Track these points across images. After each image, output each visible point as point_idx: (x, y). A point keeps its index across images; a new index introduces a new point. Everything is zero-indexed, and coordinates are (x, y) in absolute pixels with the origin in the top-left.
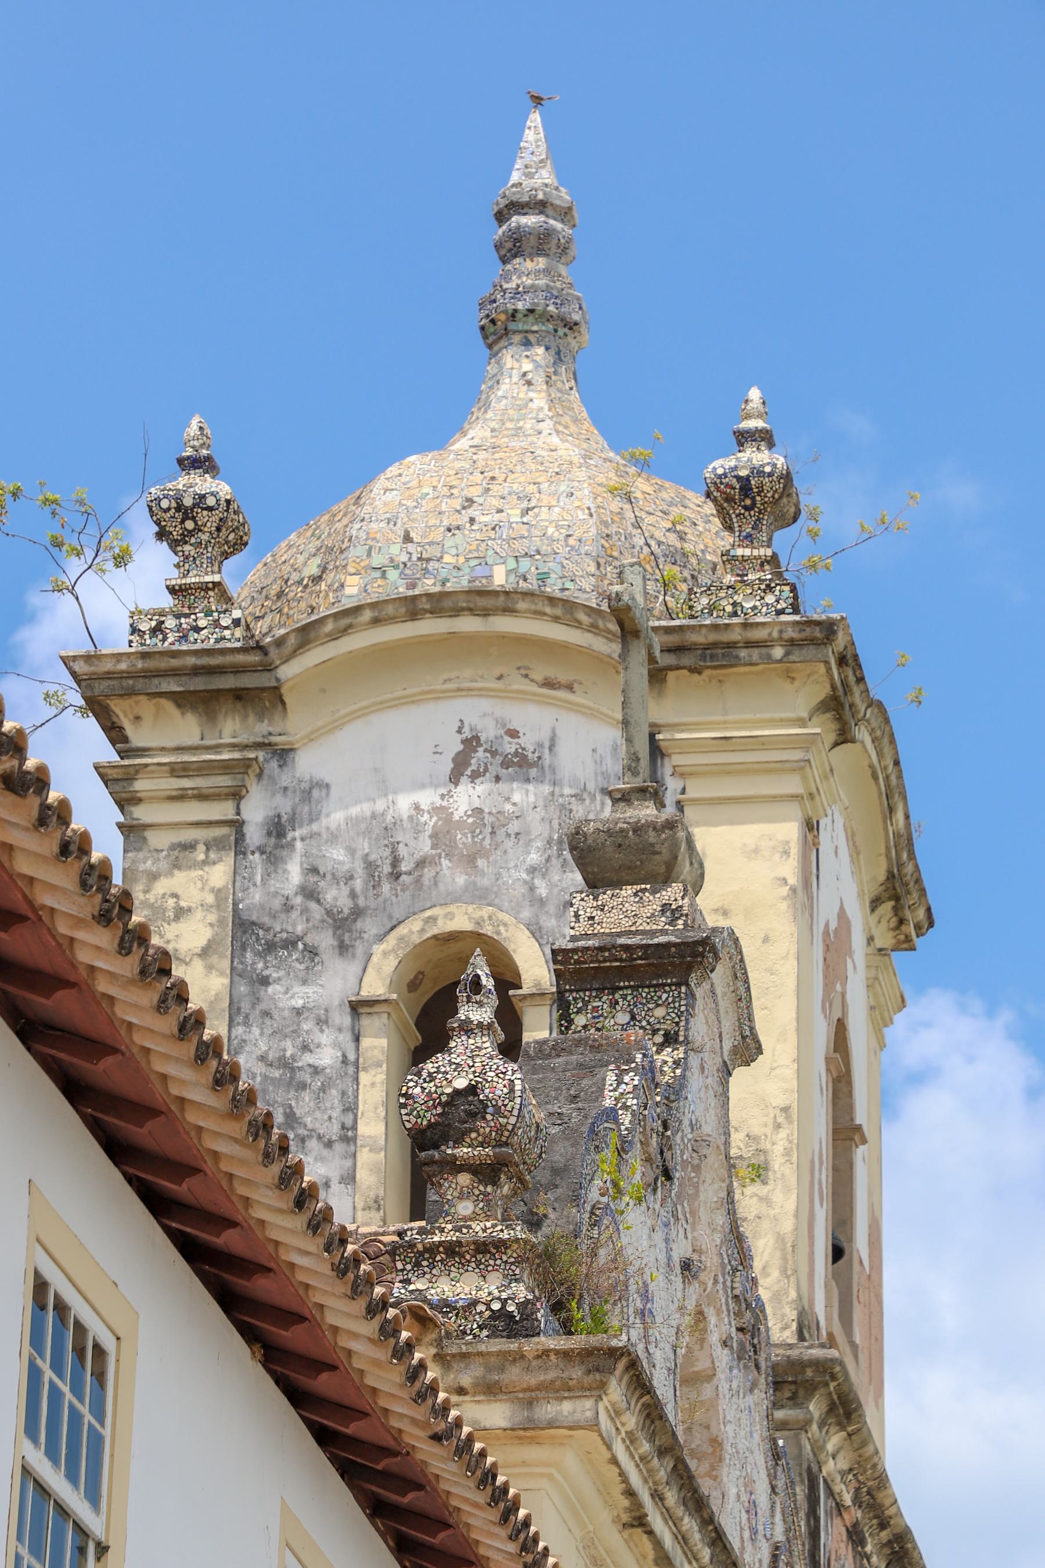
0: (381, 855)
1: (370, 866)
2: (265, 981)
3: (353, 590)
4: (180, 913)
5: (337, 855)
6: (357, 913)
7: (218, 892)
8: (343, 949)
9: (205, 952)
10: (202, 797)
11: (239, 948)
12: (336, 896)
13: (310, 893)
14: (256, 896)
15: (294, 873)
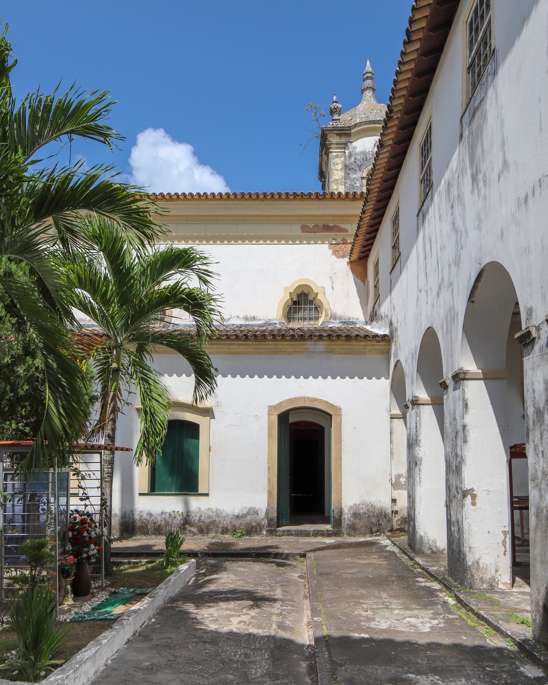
0: (365, 157)
1: (363, 159)
2: (349, 174)
3: (358, 121)
4: (337, 164)
5: (359, 157)
6: (362, 165)
7: (342, 161)
8: (360, 170)
9: (341, 170)
10: (340, 148)
11: (345, 169)
12: (358, 163)
13: (355, 162)
14: (348, 162)
15: (353, 159)
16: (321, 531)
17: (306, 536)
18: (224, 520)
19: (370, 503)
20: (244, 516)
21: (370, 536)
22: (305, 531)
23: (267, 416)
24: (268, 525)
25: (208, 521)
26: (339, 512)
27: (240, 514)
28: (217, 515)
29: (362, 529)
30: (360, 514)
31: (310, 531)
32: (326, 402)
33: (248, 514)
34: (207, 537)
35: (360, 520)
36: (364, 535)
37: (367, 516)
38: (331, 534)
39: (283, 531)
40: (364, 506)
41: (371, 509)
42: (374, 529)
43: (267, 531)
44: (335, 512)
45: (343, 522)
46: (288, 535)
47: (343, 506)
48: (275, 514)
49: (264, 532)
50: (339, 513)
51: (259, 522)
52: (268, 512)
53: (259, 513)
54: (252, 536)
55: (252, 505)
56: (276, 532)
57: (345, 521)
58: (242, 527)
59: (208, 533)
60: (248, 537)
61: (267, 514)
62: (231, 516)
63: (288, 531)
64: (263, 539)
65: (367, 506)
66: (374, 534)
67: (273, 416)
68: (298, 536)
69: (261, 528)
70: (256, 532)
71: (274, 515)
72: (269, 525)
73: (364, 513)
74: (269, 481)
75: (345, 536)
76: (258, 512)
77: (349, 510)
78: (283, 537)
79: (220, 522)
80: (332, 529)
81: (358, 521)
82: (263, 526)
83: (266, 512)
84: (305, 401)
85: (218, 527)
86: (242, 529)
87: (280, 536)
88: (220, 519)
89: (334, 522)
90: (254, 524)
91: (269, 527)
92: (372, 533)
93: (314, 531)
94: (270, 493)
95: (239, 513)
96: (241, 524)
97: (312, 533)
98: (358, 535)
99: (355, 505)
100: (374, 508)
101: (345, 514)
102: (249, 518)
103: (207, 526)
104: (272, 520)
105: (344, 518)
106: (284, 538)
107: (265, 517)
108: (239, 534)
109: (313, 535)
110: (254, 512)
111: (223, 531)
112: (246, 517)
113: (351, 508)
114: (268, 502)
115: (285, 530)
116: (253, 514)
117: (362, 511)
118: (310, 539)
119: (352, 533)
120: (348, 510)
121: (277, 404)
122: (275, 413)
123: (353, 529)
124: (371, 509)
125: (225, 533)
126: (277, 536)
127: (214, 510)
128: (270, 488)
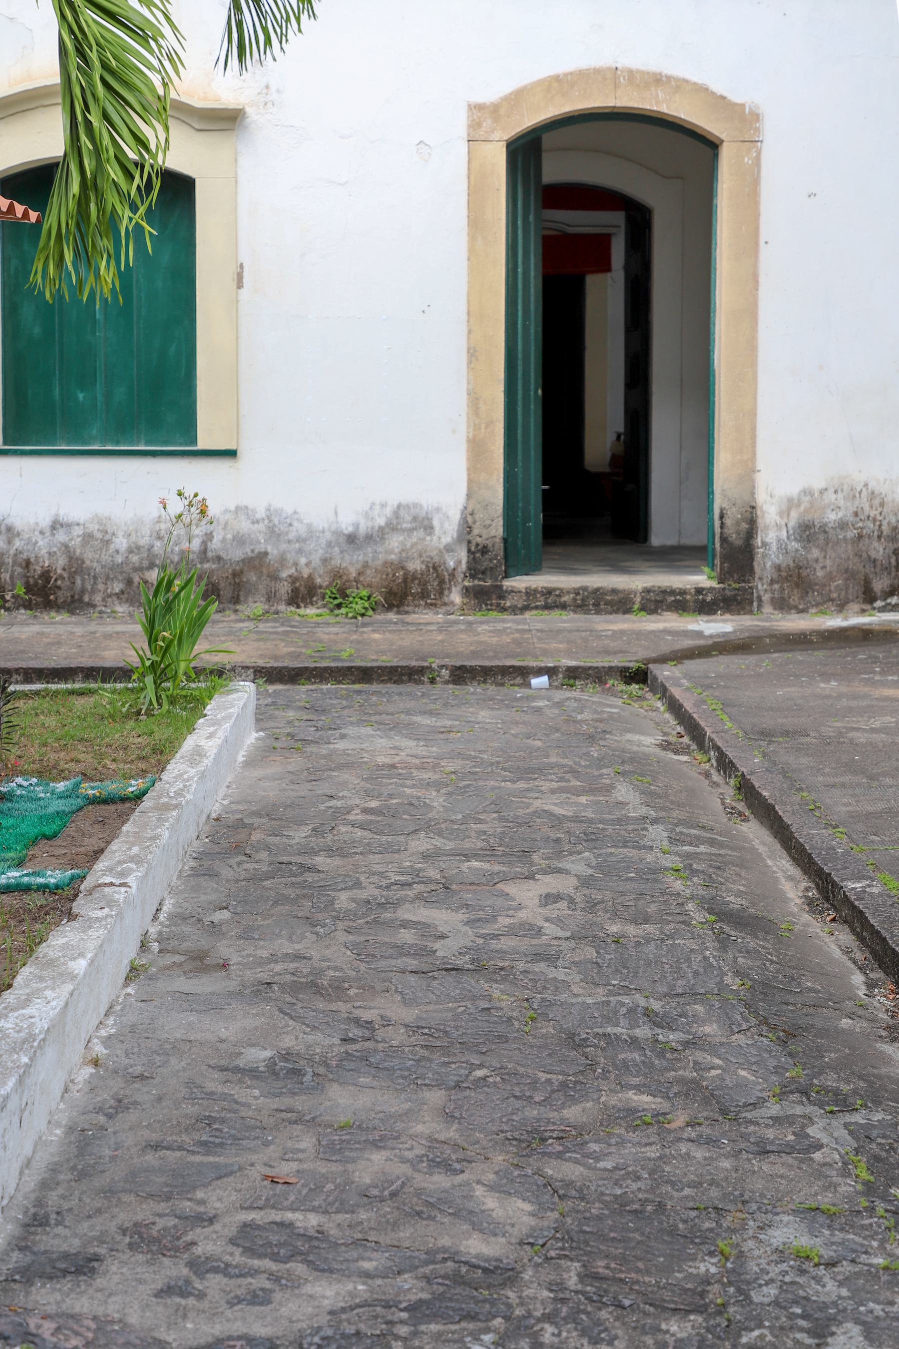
16: (673, 592)
17: (616, 612)
18: (300, 551)
19: (866, 485)
20: (376, 537)
21: (863, 611)
22: (614, 591)
23: (463, 147)
24: (469, 568)
25: (236, 554)
26: (743, 520)
27: (362, 530)
28: (273, 533)
29: (833, 585)
30: (824, 529)
31: (630, 592)
32: (702, 90)
33: (391, 527)
34: (233, 617)
35: (823, 550)
36: (841, 607)
37: (851, 534)
38: (714, 602)
39: (530, 593)
40: (840, 495)
42: (879, 585)
43: (467, 591)
44: (728, 522)
45: (758, 558)
46: (547, 607)
47: (761, 497)
48: (498, 530)
49: (456, 597)
50: (745, 526)
51: (436, 559)
52: (470, 519)
53: (436, 523)
54: (407, 613)
55: (408, 495)
56: (502, 597)
57: (764, 556)
58: (370, 576)
59: (236, 600)
60: (392, 616)
61: (466, 527)
62: (328, 535)
63: (549, 592)
64: (456, 622)
65: (853, 495)
66: (879, 604)
67: (489, 146)
68: (587, 612)
69: (442, 582)
70: (424, 595)
71: (493, 533)
72: (474, 571)
73: (843, 525)
74: (475, 401)
75: (767, 609)
76: (430, 519)
77: (785, 513)
78: (528, 615)
79: (282, 560)
80: (714, 584)
81: (816, 553)
82: (452, 575)
84: (616, 86)
85: (275, 577)
86: (370, 586)
87: (514, 610)
88: (284, 546)
89: (725, 558)
90: (415, 566)
91: (473, 577)
92: (869, 597)
93: (647, 591)
94: (476, 448)
95: (357, 526)
96: (366, 565)
97: (638, 599)
98: (817, 605)
99: (807, 492)
100: (882, 504)
101: (767, 527)
102: (395, 542)
103: (235, 574)
104: (484, 550)
105: (765, 544)
106: (535, 620)
107: (459, 540)
108: (359, 606)
109: (643, 609)
110: (415, 519)
111: (295, 591)
112: (383, 538)
113: (791, 503)
114: (470, 481)
115: (536, 590)
116: (412, 530)
117: (832, 517)
118: (634, 622)
119: (794, 599)
120: (781, 514)
121: (506, 99)
122: (496, 136)
123: (797, 585)
125: (303, 599)
126: (503, 610)
127: (261, 513)
128: (477, 427)
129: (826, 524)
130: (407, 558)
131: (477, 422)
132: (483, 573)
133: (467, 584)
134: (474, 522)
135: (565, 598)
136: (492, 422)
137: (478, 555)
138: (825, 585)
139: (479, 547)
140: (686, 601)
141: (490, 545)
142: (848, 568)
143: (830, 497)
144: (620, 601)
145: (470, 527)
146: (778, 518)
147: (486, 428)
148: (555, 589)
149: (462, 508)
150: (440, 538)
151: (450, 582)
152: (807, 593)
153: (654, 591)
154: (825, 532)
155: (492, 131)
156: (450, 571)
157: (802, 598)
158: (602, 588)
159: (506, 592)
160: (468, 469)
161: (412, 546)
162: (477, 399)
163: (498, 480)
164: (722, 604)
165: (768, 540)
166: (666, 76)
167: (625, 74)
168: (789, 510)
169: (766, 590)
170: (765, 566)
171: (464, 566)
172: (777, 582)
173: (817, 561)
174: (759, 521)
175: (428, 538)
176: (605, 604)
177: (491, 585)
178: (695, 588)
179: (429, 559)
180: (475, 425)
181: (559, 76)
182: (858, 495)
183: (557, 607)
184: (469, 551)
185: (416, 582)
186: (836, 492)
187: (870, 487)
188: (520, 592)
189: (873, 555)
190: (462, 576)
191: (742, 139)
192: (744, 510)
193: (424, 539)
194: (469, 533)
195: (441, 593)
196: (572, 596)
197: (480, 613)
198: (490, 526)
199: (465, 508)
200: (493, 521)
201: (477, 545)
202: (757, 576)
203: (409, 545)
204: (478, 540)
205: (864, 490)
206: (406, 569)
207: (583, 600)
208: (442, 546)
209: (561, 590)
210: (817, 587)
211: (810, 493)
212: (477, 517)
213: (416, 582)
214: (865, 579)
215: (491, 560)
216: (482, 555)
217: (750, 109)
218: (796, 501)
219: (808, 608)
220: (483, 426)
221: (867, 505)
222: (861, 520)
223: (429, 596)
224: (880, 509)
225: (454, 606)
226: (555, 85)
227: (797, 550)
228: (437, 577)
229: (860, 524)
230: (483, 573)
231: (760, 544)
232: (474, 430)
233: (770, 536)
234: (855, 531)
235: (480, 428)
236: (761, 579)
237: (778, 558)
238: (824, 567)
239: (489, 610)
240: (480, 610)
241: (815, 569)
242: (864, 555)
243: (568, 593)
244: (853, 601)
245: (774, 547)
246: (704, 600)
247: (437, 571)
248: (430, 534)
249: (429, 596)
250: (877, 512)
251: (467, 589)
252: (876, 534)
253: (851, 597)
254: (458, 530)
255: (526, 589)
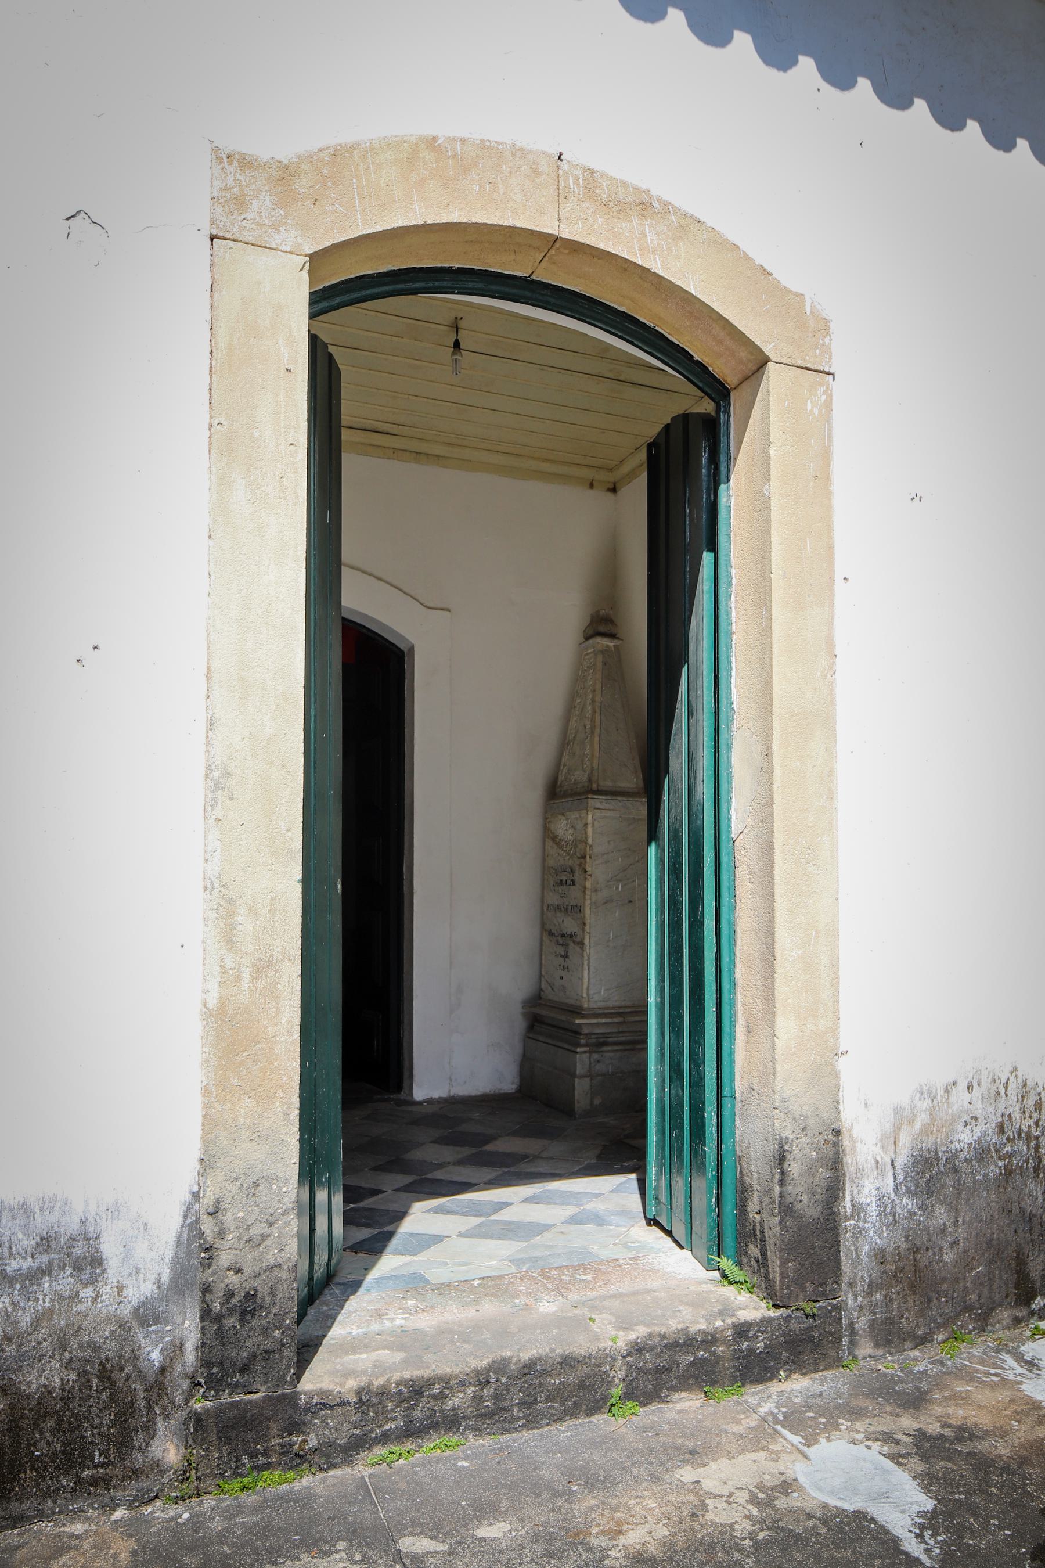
17: (572, 1413)
22: (568, 1362)
24: (205, 1362)
37: (994, 1168)
38: (770, 1352)
40: (977, 1092)
41: (1017, 1116)
46: (412, 1432)
50: (823, 1173)
51: (111, 1349)
52: (208, 1226)
53: (110, 1249)
56: (295, 1427)
57: (858, 1232)
69: (125, 1411)
73: (982, 1152)
76: (91, 1239)
83: (192, 1228)
91: (215, 1384)
93: (638, 1349)
98: (944, 1325)
105: (858, 1209)
107: (178, 1286)
115: (383, 1393)
116: (34, 1276)
117: (965, 1138)
120: (883, 1141)
124: (1017, 1116)
128: (229, 978)
129: (955, 1155)
130: (21, 1358)
131: (229, 963)
132: (245, 1369)
133: (198, 1406)
134: (221, 1234)
135: (457, 1401)
136: (271, 962)
137: (231, 1322)
138: (957, 1280)
139: (234, 1301)
140: (717, 1359)
141: (264, 1291)
142: (992, 1240)
143: (960, 1097)
144: (581, 1386)
145: (207, 1250)
146: (878, 1150)
147: (254, 979)
148: (430, 1382)
149: (188, 1197)
150: (120, 1289)
151: (149, 1407)
152: (930, 1300)
153: (652, 1348)
154: (956, 1170)
155: (276, 227)
156: (151, 1379)
157: (921, 1313)
158: (539, 1359)
159: (307, 1410)
160: (206, 1091)
161: (37, 1322)
162: (231, 902)
163: (286, 1114)
164: (785, 1354)
165: (862, 1200)
166: (659, 200)
167: (578, 172)
168: (897, 1129)
169: (861, 1307)
170: (858, 1256)
171: (190, 1356)
172: (880, 1287)
173: (943, 1230)
174: (848, 1159)
175: (87, 1293)
176: (548, 1399)
177: (267, 1399)
178: (734, 1326)
179: (87, 1354)
180: (224, 971)
181: (435, 139)
182: (1002, 1091)
183: (435, 1426)
184: (206, 1313)
185: (49, 1424)
186: (970, 1087)
187: (1020, 1073)
188: (343, 1404)
189: (1028, 1206)
190: (186, 1384)
191: (800, 363)
192: (821, 1139)
193: (75, 1297)
194: (206, 1264)
195: (123, 1443)
196: (470, 1390)
197: (236, 1485)
198: (264, 1238)
199: (196, 1196)
200: (271, 1224)
201: (230, 1294)
202: (845, 1279)
203: (25, 1319)
204: (232, 1279)
205: (1012, 1079)
206: (18, 1393)
207: (496, 1397)
208: (126, 1311)
209: (445, 1380)
210: (945, 1287)
211: (930, 1092)
212: (228, 1218)
213: (49, 1424)
214: (1018, 1257)
215: (265, 1331)
216: (243, 1321)
217: (812, 306)
218: (907, 1112)
219: (932, 1333)
220: (246, 974)
221: (1017, 1109)
222: (1008, 1139)
223: (86, 1460)
224: (1035, 1115)
225: (162, 1473)
226: (427, 155)
227: (912, 1214)
228: (112, 1399)
229: (1008, 1149)
230: (245, 1369)
231: (849, 1211)
232: (222, 983)
233: (866, 1191)
234: (1000, 1164)
235: (238, 979)
236: (851, 1284)
237: (880, 1235)
238: (955, 1243)
239: (259, 1469)
240: (236, 1474)
241: (941, 1249)
242: (1016, 1210)
243: (462, 1384)
244: (1001, 1305)
245: (873, 1211)
246: (751, 1351)
247: (113, 1383)
248: (93, 1281)
249: (86, 1460)
250: (1031, 1122)
251: (199, 1420)
252: (1031, 1164)
253: (997, 1297)
254: (174, 1261)
255: (358, 1393)
